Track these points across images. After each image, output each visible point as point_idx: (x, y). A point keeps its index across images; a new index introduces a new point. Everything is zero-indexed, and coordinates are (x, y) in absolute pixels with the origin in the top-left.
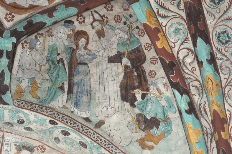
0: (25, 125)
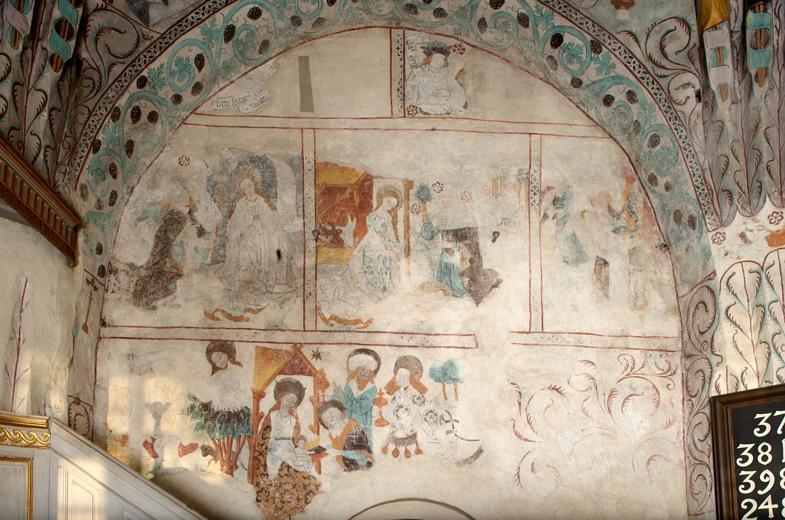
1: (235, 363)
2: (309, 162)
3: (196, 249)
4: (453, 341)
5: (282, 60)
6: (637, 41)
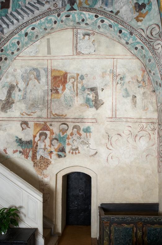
0: (85, 22)
1: (28, 127)
2: (49, 69)
3: (18, 95)
4: (90, 121)
5: (42, 40)
6: (144, 31)
